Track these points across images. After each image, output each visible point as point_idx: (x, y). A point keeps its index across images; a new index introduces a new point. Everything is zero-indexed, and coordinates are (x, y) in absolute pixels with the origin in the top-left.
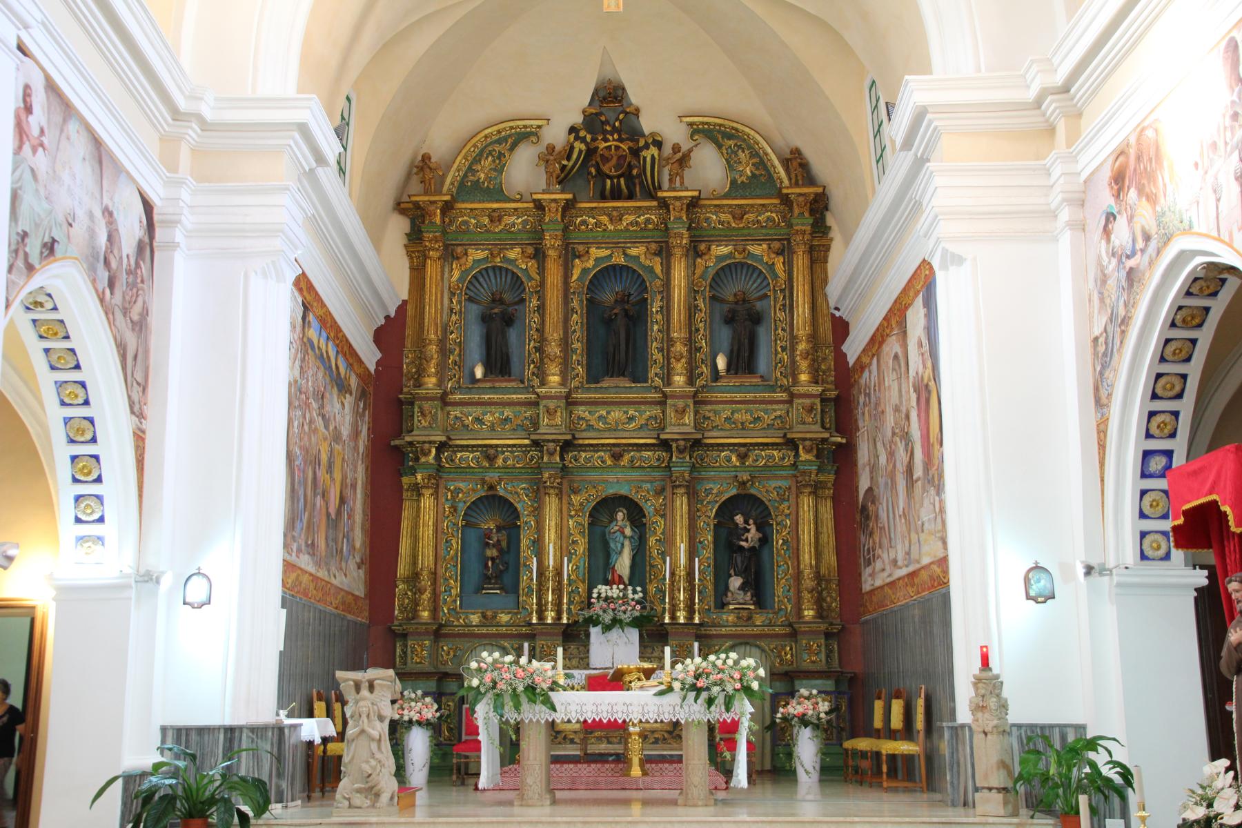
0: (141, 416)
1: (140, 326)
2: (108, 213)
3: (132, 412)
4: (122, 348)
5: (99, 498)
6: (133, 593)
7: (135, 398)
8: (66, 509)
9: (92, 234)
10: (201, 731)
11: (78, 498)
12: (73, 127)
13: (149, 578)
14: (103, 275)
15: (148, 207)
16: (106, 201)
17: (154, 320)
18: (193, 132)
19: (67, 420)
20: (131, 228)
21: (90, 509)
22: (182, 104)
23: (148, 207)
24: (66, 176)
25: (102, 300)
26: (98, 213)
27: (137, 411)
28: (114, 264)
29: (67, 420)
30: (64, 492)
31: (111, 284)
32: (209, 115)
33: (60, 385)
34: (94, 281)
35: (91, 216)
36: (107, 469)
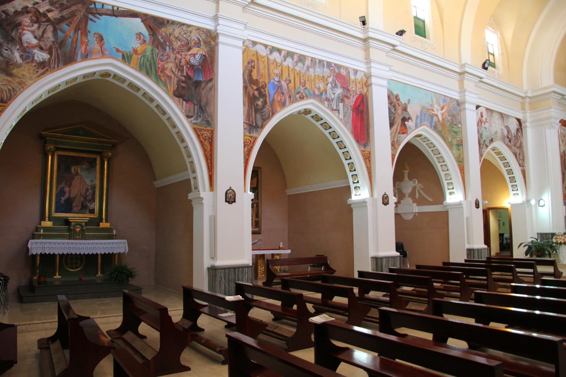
0: (523, 166)
1: (521, 147)
2: (507, 127)
3: (520, 166)
4: (515, 154)
5: (516, 185)
6: (526, 205)
7: (521, 163)
8: (510, 188)
9: (503, 133)
10: (546, 234)
11: (512, 186)
12: (494, 114)
13: (528, 201)
14: (507, 140)
15: (519, 120)
16: (506, 124)
17: (524, 145)
18: (528, 100)
19: (507, 170)
20: (514, 126)
21: (514, 187)
22: (523, 95)
23: (519, 120)
24: (494, 125)
25: (507, 145)
26: (504, 128)
27: (522, 165)
28: (510, 137)
29: (507, 170)
30: (510, 185)
31: (510, 141)
32: (529, 95)
33: (504, 163)
34: (505, 143)
35: (502, 129)
36: (516, 179)
